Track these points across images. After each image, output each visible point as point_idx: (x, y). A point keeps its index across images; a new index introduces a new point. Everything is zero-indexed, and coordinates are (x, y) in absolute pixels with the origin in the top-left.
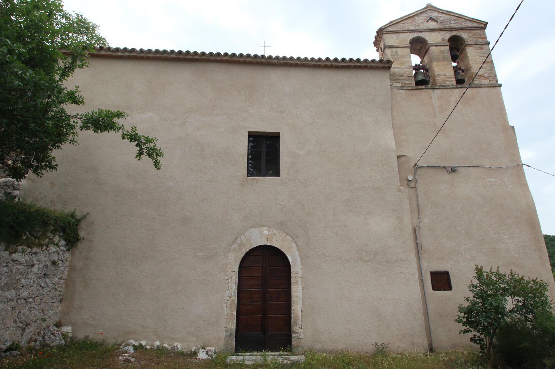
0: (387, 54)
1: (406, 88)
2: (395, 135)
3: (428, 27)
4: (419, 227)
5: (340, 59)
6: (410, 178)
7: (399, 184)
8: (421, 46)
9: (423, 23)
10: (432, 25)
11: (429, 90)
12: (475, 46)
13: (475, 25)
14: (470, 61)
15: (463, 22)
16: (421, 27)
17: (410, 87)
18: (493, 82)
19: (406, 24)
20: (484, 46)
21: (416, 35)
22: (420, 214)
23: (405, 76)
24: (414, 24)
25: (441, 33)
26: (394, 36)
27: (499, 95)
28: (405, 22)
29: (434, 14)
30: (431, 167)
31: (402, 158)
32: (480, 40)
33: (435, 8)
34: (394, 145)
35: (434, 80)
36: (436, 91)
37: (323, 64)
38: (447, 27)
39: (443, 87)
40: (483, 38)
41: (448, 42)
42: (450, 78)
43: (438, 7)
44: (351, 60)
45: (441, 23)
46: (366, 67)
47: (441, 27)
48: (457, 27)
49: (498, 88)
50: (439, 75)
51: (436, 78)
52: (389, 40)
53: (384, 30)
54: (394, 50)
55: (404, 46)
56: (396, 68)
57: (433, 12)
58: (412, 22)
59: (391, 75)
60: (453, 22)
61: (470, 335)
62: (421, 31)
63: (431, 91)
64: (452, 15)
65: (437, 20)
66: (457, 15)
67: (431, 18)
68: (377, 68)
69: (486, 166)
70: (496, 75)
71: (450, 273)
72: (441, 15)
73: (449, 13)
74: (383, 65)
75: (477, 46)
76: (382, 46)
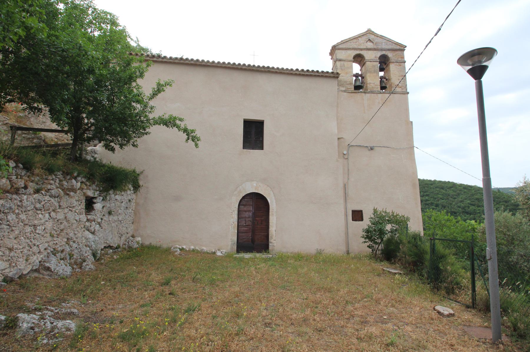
0: (338, 66)
1: (348, 91)
2: (338, 124)
3: (366, 46)
4: (348, 183)
5: (305, 70)
6: (345, 152)
7: (337, 157)
8: (361, 59)
9: (364, 44)
10: (370, 45)
11: (362, 94)
12: (396, 63)
13: (398, 47)
14: (391, 74)
15: (390, 44)
16: (362, 47)
17: (350, 91)
18: (404, 90)
19: (352, 43)
20: (402, 64)
21: (358, 52)
22: (349, 176)
23: (348, 83)
24: (357, 43)
25: (375, 52)
26: (343, 52)
27: (406, 100)
28: (351, 41)
29: (372, 37)
30: (358, 146)
31: (341, 139)
32: (400, 59)
33: (373, 32)
34: (336, 131)
35: (367, 86)
36: (367, 94)
37: (294, 73)
38: (379, 48)
39: (372, 92)
40: (402, 58)
41: (379, 59)
42: (377, 86)
43: (375, 32)
44: (313, 71)
45: (375, 44)
46: (322, 76)
47: (375, 47)
48: (386, 48)
49: (406, 95)
50: (370, 83)
51: (368, 86)
52: (340, 54)
53: (336, 47)
54: (342, 62)
55: (349, 60)
56: (342, 76)
57: (371, 35)
58: (356, 42)
59: (338, 81)
60: (383, 44)
61: (368, 244)
62: (361, 50)
63: (364, 94)
64: (384, 39)
65: (373, 41)
66: (387, 39)
67: (369, 39)
68: (330, 77)
69: (392, 147)
70: (406, 85)
71: (363, 212)
72: (376, 38)
73: (382, 37)
74: (334, 76)
75: (397, 64)
76: (334, 57)
